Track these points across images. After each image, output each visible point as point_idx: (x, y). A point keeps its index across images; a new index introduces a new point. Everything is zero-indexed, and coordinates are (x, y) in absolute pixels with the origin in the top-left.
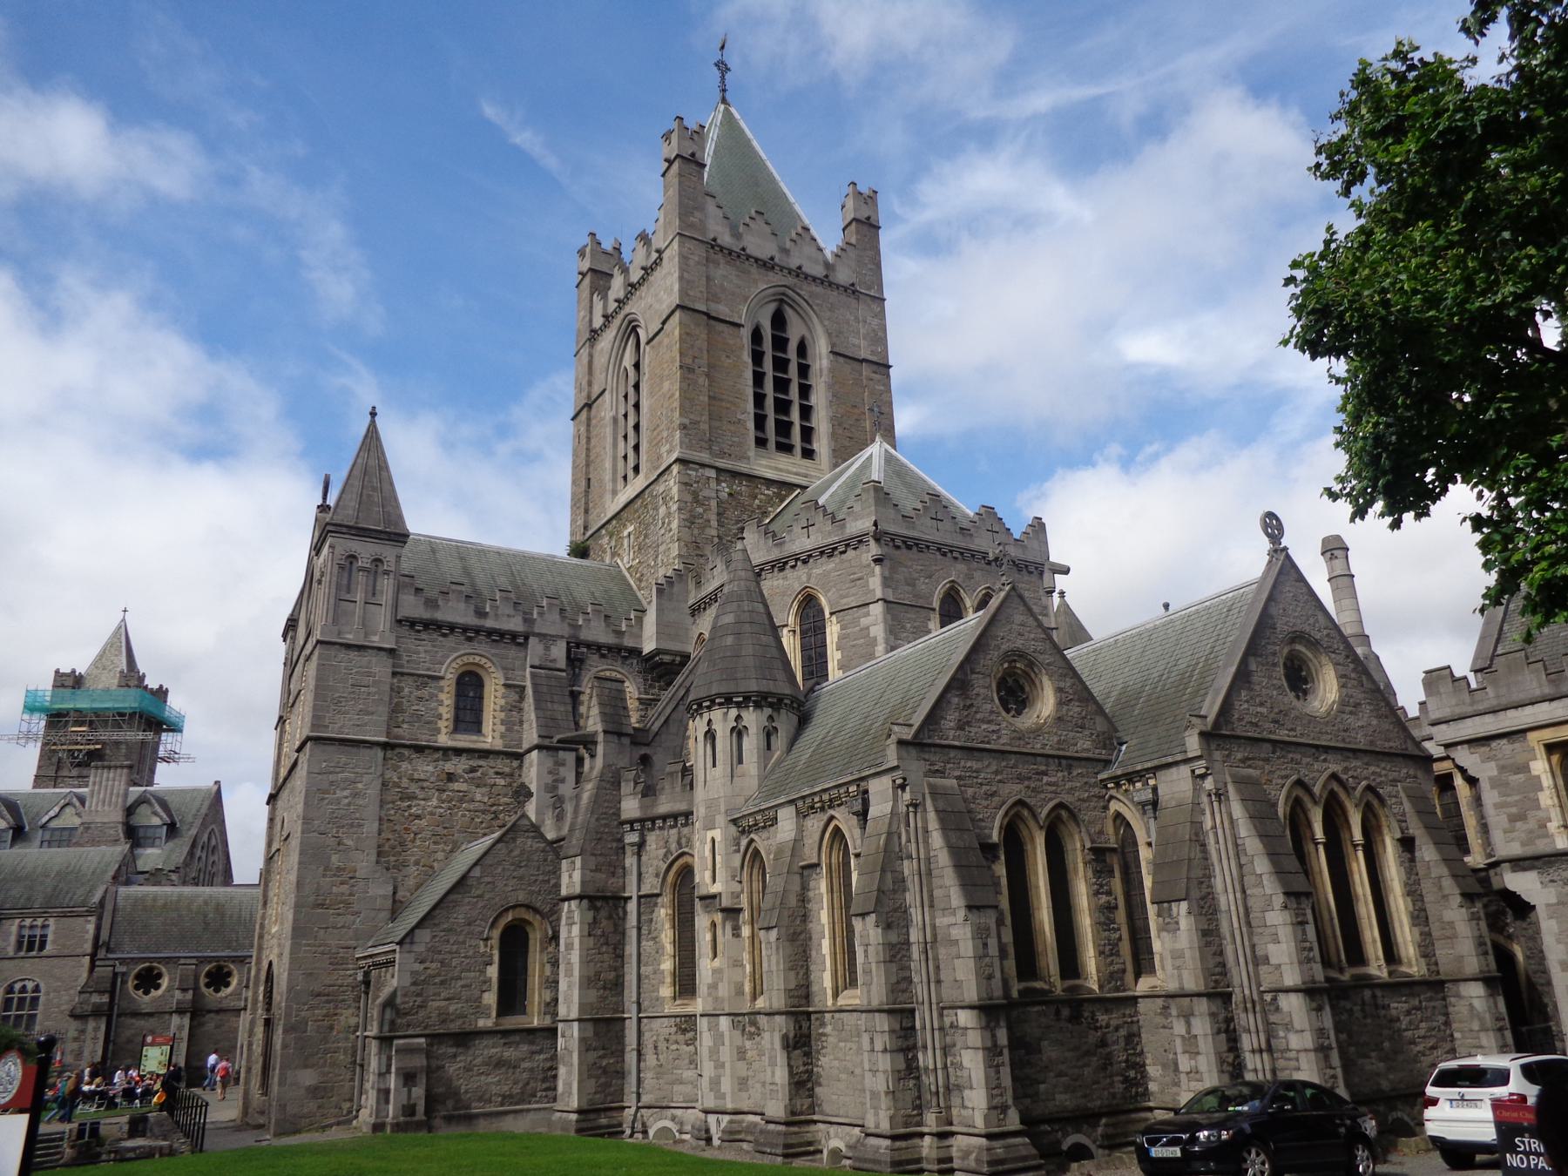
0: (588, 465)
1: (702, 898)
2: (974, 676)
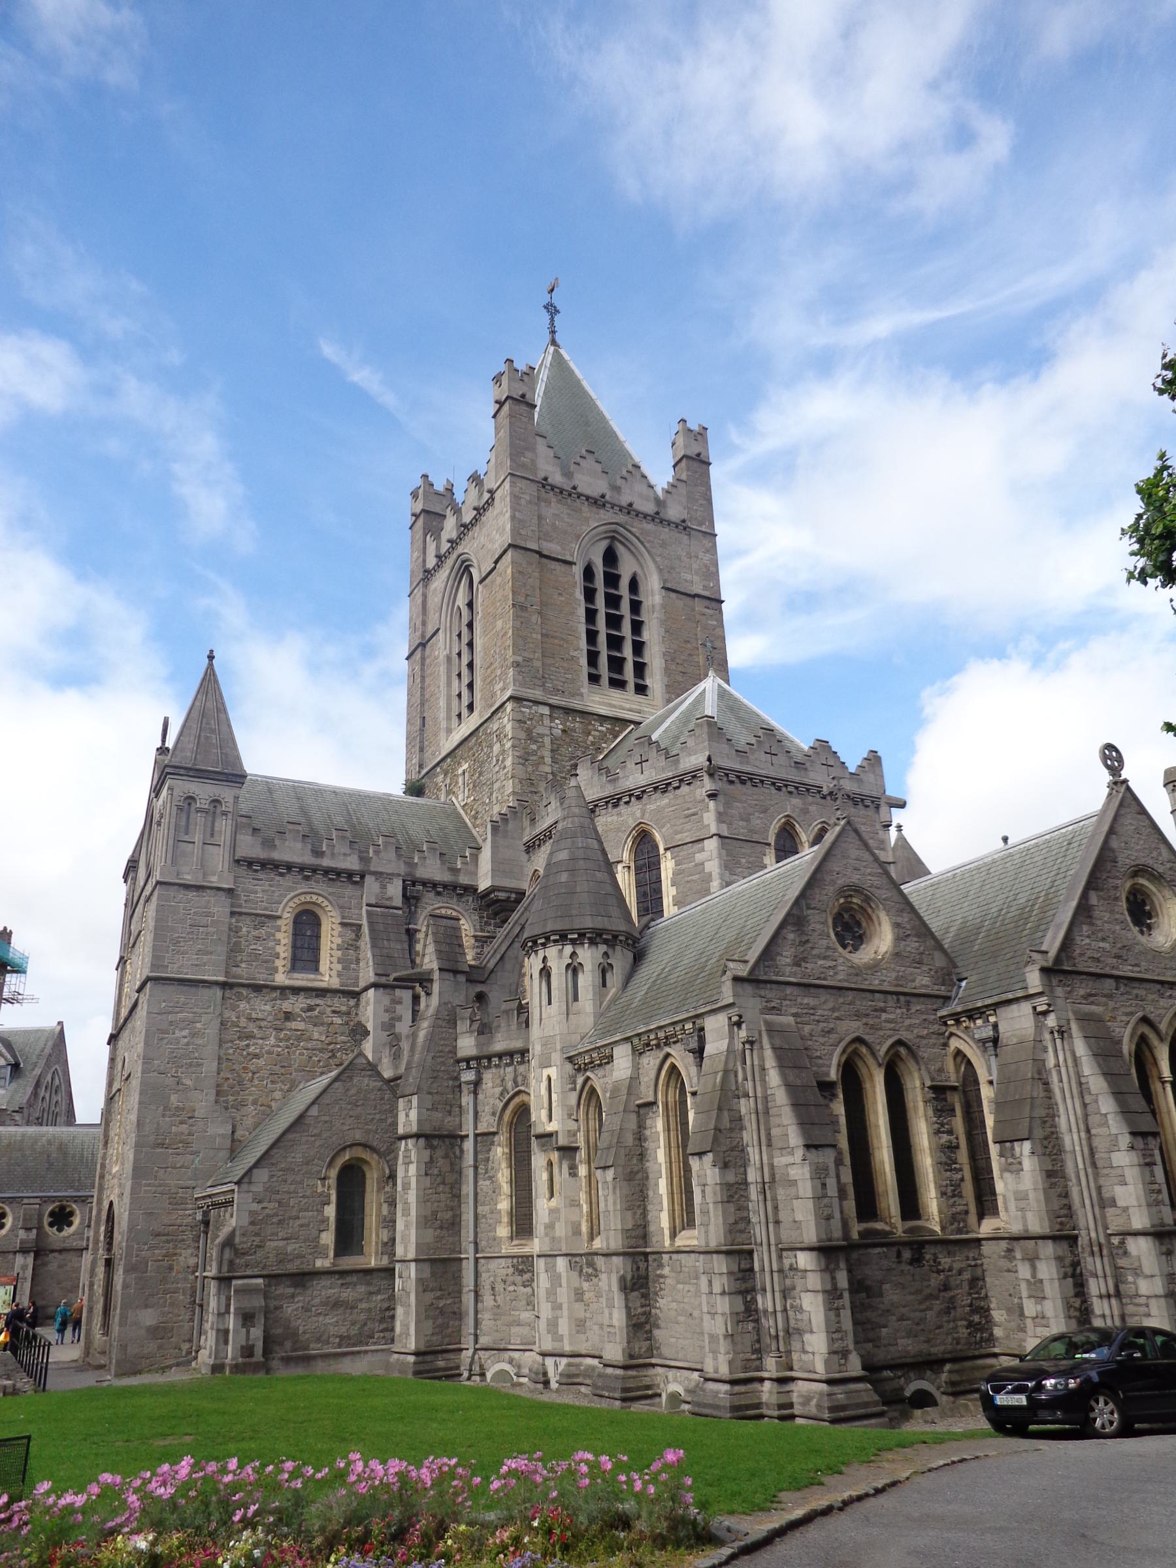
0: (422, 704)
1: (538, 1137)
2: (810, 912)
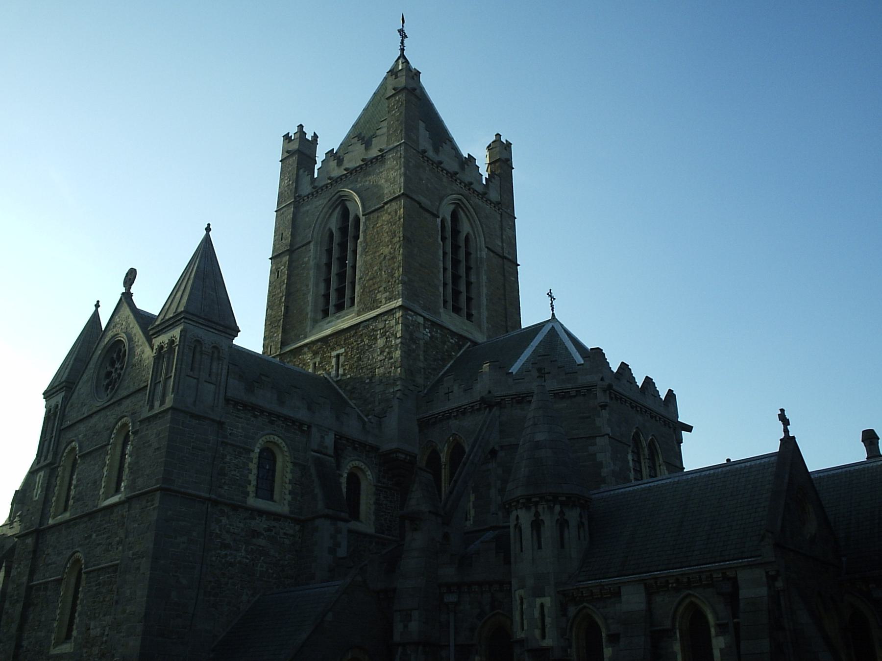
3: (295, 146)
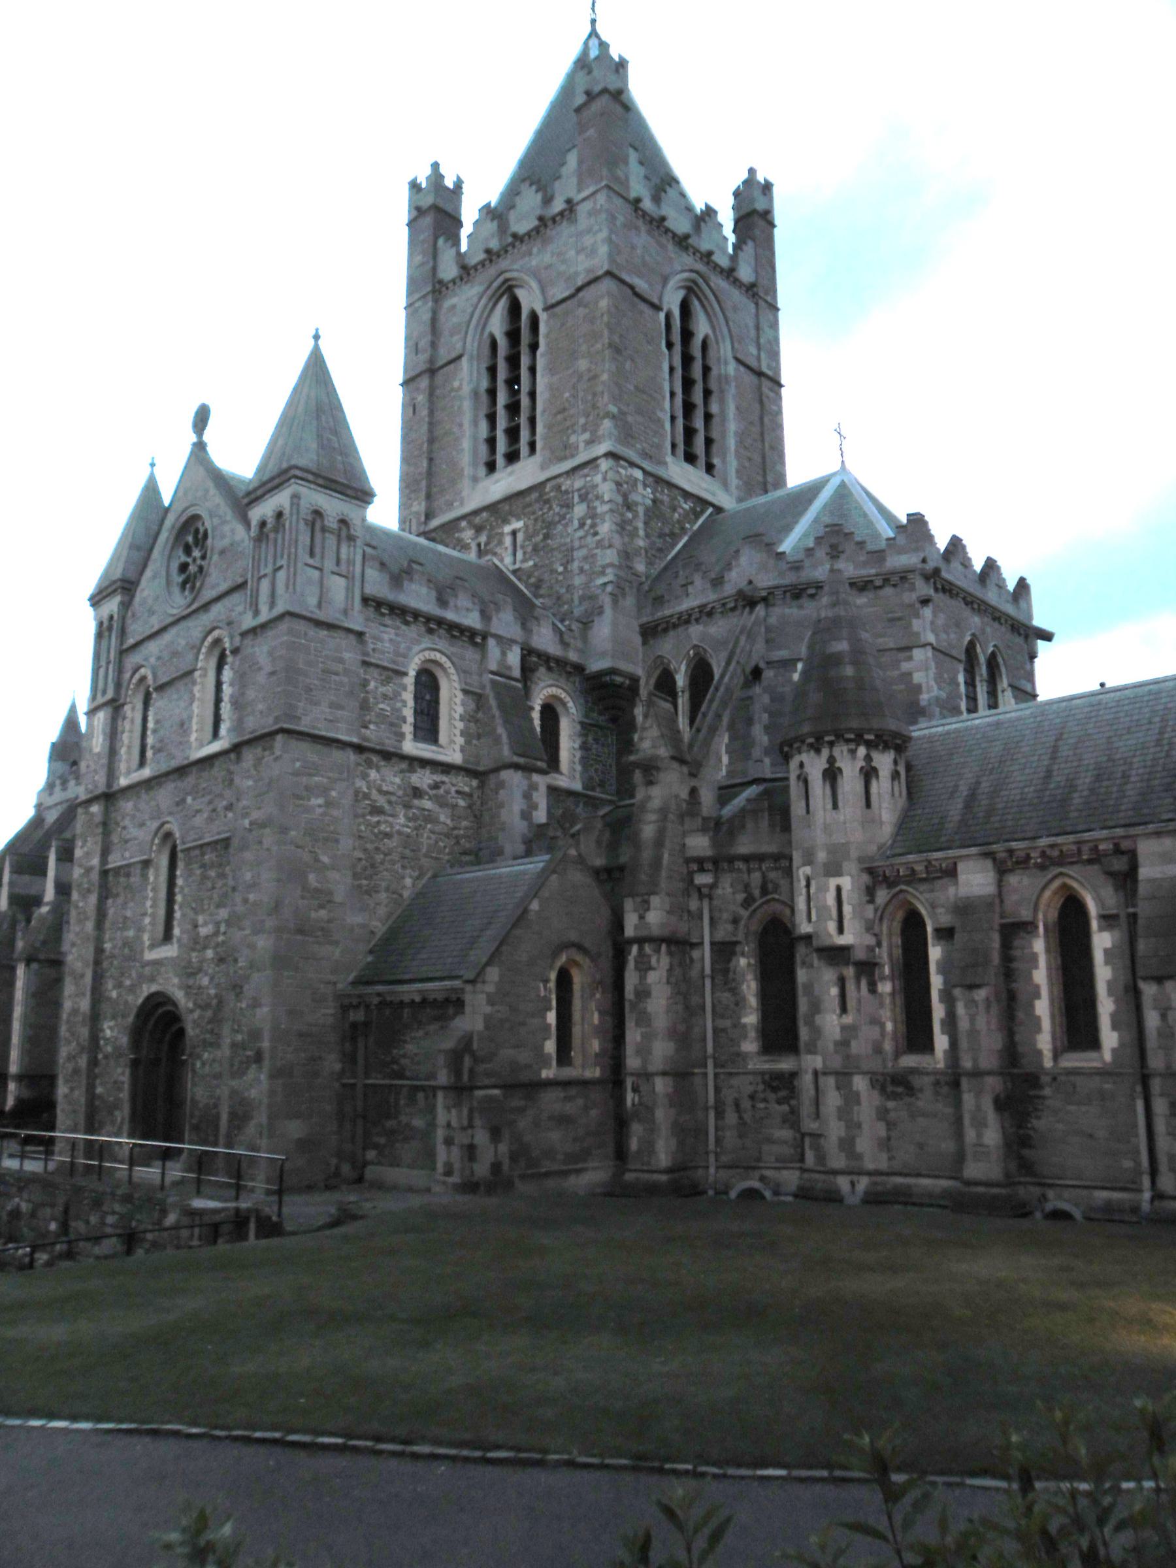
0: (432, 440)
3: (427, 201)
